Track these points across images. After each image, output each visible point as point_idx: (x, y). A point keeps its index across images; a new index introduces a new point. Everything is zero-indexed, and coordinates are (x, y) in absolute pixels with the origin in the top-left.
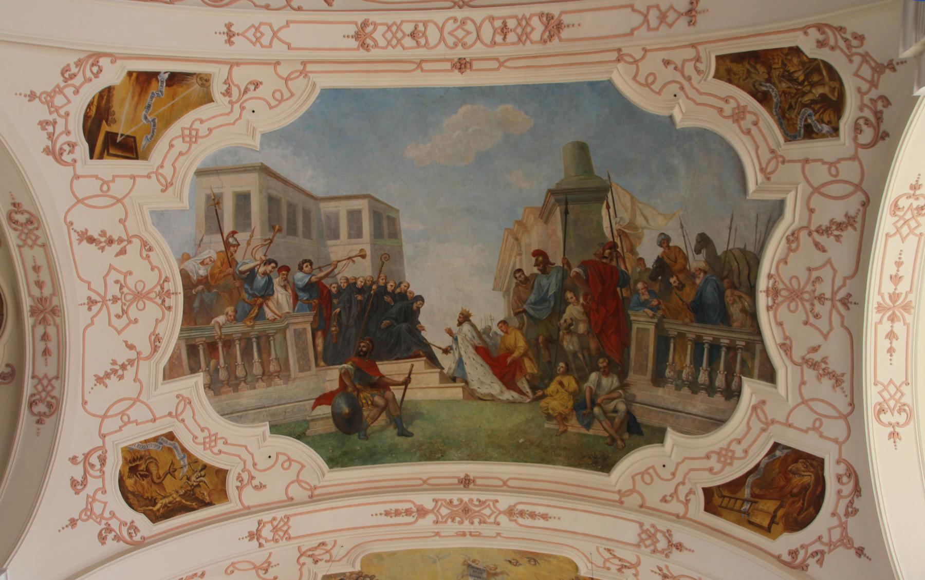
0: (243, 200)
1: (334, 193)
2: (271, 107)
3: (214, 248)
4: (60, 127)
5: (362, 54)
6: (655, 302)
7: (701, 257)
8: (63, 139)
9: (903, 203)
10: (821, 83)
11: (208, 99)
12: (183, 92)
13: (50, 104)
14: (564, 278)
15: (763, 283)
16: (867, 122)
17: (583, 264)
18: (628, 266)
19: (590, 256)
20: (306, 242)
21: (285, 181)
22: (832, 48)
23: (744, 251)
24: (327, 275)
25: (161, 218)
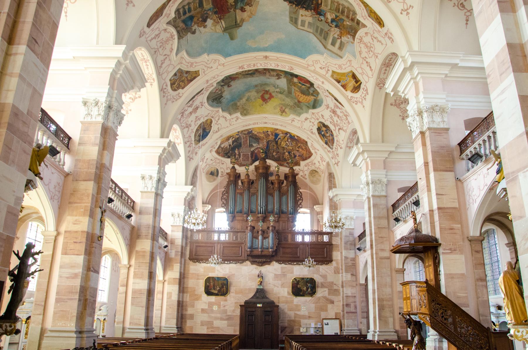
0: (333, 44)
1: (308, 33)
2: (319, 61)
3: (344, 39)
4: (363, 95)
5: (292, 66)
6: (205, 12)
7: (193, 28)
8: (365, 92)
9: (153, 81)
10: (176, 86)
11: (333, 72)
12: (338, 77)
13: (362, 101)
14: (236, 7)
15: (176, 37)
16: (165, 89)
17: (229, 12)
18: (215, 17)
19: (227, 15)
20: (318, 25)
21: (321, 42)
22: (176, 95)
23: (183, 37)
24: (314, 15)
25: (354, 56)
